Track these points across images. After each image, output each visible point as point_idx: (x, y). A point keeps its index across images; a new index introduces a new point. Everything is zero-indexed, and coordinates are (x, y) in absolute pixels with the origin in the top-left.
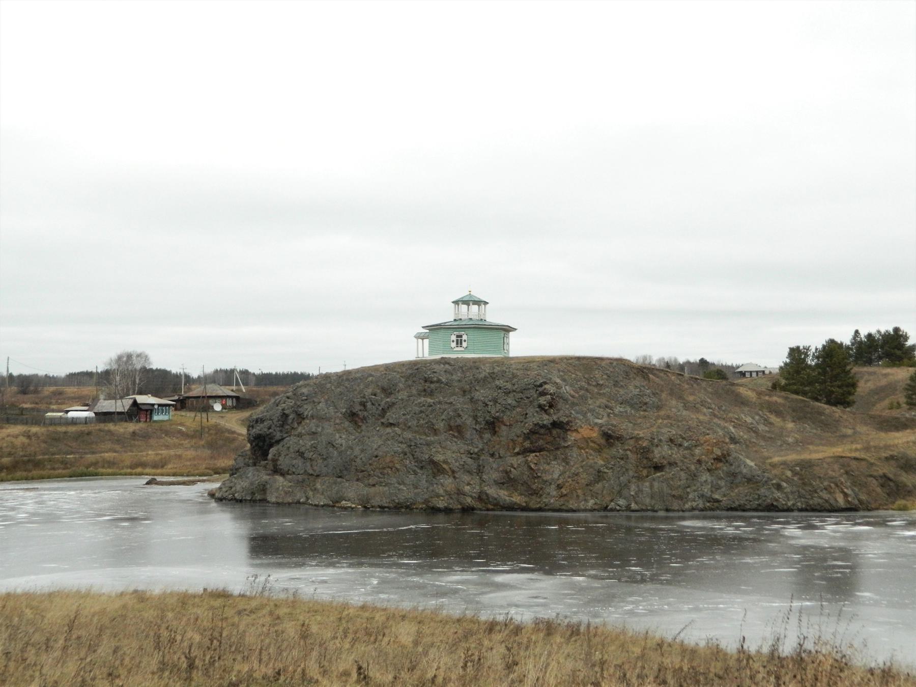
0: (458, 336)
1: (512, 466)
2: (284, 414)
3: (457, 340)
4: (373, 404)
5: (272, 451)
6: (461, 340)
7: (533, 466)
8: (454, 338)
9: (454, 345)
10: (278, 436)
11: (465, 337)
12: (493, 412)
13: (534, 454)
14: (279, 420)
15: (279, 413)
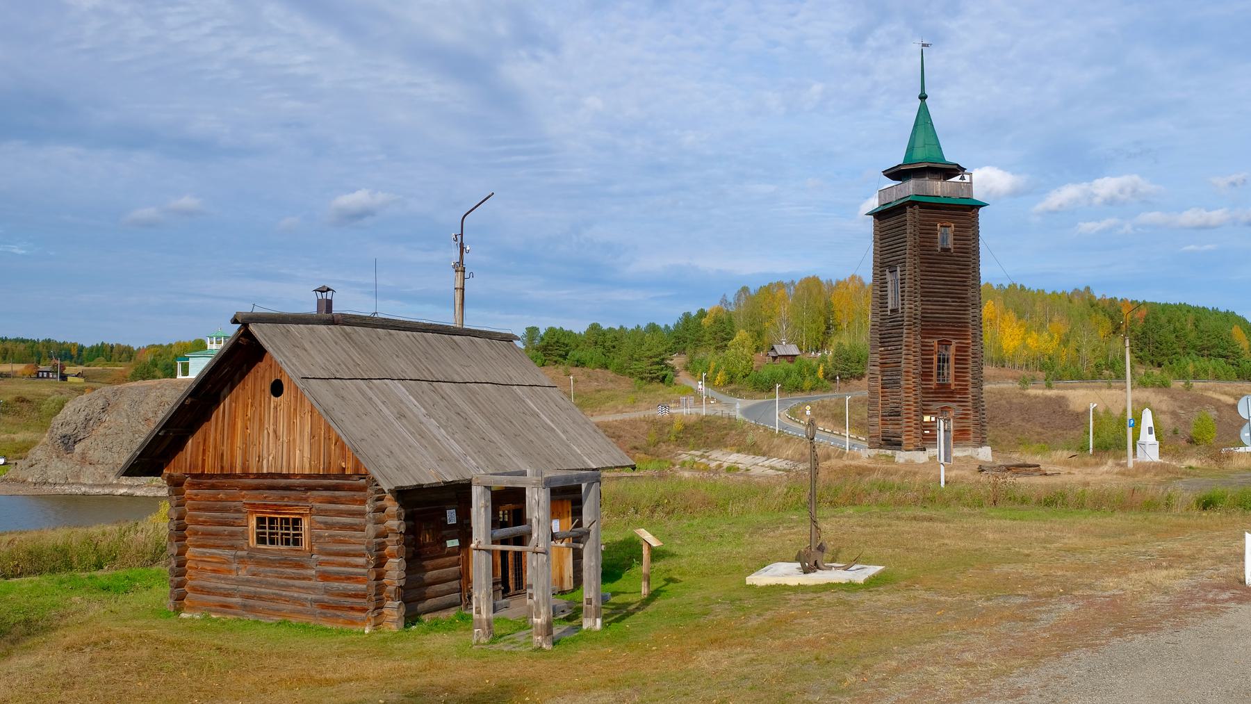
5: (78, 448)
14: (82, 424)
15: (82, 417)
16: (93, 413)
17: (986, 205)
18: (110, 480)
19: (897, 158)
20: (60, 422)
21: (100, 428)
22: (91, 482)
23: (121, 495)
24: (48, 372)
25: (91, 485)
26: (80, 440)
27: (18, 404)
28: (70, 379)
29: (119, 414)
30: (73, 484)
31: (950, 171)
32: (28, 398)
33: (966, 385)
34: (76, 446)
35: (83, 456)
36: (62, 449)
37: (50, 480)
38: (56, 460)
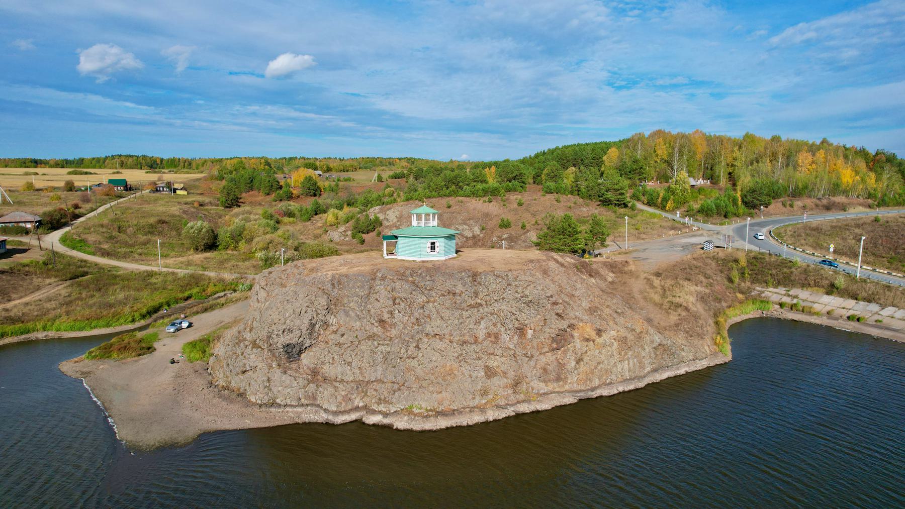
0: (433, 243)
3: (432, 247)
4: (399, 312)
5: (306, 359)
6: (434, 246)
7: (561, 361)
8: (430, 245)
15: (307, 322)
16: (318, 314)
18: (356, 403)
22: (335, 409)
23: (374, 425)
24: (163, 187)
25: (336, 412)
26: (306, 348)
27: (160, 225)
28: (178, 192)
30: (308, 405)
32: (167, 219)
34: (303, 356)
35: (315, 372)
37: (278, 401)
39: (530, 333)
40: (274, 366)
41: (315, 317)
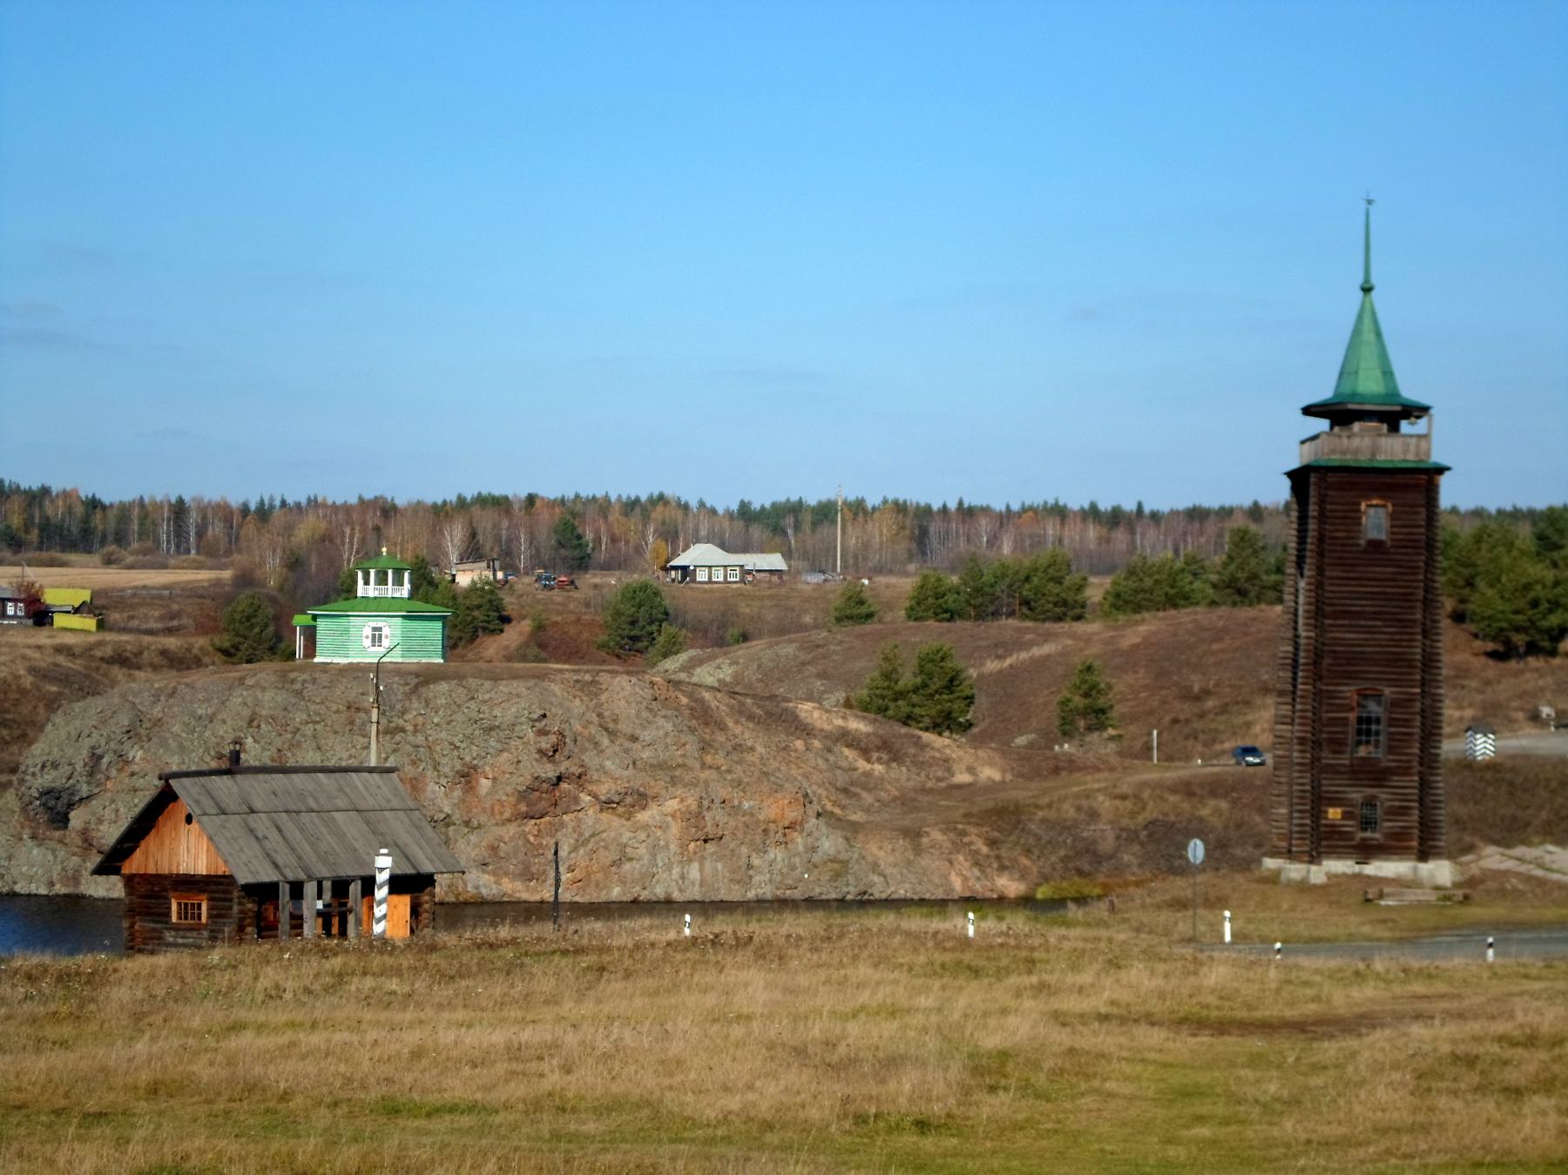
0: (374, 629)
1: (501, 839)
2: (93, 754)
3: (374, 636)
5: (77, 818)
6: (380, 636)
7: (532, 839)
8: (368, 631)
9: (368, 642)
10: (84, 790)
11: (386, 631)
12: (468, 759)
13: (533, 822)
15: (85, 753)
17: (1448, 469)
19: (1323, 392)
20: (39, 761)
21: (123, 775)
26: (81, 800)
29: (164, 743)
31: (1396, 414)
33: (1410, 761)
36: (43, 818)
38: (30, 843)
39: (485, 784)
40: (25, 837)
41: (103, 743)
